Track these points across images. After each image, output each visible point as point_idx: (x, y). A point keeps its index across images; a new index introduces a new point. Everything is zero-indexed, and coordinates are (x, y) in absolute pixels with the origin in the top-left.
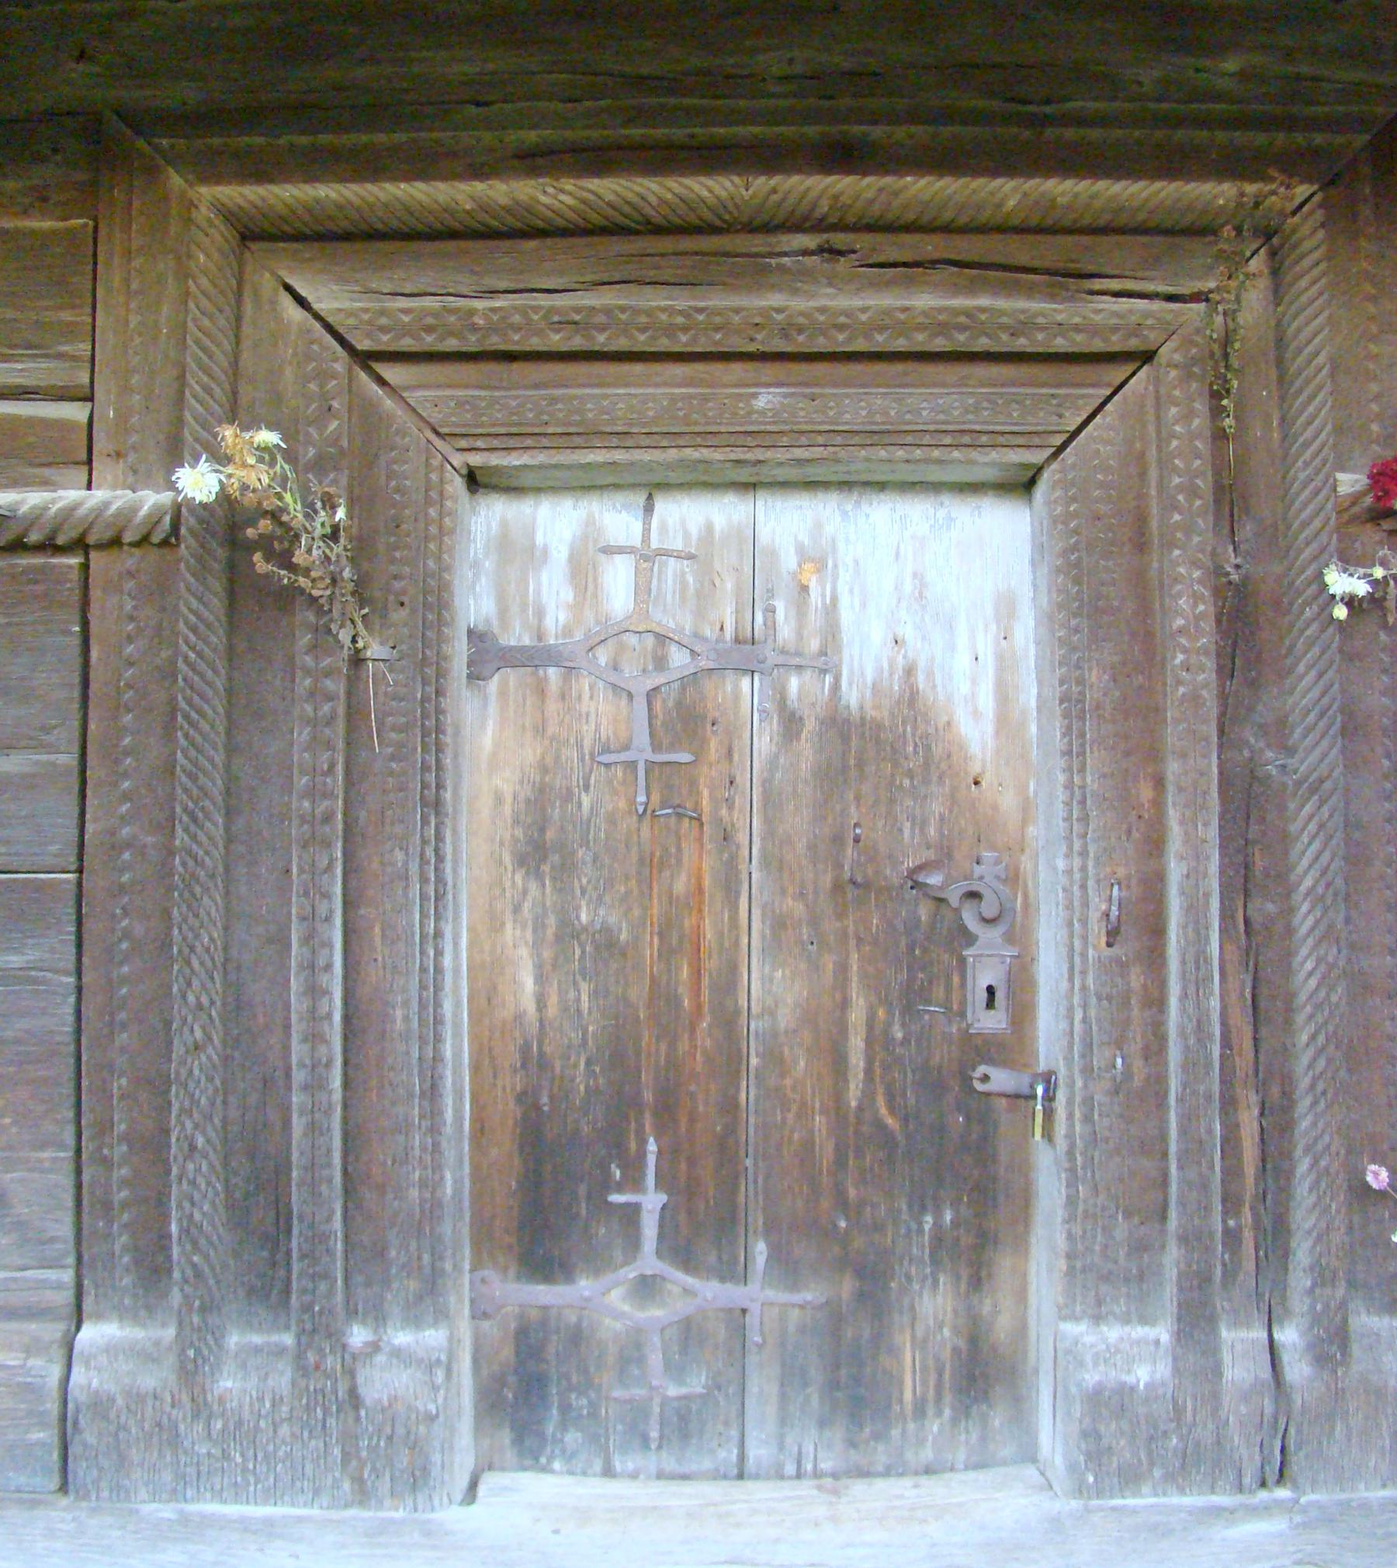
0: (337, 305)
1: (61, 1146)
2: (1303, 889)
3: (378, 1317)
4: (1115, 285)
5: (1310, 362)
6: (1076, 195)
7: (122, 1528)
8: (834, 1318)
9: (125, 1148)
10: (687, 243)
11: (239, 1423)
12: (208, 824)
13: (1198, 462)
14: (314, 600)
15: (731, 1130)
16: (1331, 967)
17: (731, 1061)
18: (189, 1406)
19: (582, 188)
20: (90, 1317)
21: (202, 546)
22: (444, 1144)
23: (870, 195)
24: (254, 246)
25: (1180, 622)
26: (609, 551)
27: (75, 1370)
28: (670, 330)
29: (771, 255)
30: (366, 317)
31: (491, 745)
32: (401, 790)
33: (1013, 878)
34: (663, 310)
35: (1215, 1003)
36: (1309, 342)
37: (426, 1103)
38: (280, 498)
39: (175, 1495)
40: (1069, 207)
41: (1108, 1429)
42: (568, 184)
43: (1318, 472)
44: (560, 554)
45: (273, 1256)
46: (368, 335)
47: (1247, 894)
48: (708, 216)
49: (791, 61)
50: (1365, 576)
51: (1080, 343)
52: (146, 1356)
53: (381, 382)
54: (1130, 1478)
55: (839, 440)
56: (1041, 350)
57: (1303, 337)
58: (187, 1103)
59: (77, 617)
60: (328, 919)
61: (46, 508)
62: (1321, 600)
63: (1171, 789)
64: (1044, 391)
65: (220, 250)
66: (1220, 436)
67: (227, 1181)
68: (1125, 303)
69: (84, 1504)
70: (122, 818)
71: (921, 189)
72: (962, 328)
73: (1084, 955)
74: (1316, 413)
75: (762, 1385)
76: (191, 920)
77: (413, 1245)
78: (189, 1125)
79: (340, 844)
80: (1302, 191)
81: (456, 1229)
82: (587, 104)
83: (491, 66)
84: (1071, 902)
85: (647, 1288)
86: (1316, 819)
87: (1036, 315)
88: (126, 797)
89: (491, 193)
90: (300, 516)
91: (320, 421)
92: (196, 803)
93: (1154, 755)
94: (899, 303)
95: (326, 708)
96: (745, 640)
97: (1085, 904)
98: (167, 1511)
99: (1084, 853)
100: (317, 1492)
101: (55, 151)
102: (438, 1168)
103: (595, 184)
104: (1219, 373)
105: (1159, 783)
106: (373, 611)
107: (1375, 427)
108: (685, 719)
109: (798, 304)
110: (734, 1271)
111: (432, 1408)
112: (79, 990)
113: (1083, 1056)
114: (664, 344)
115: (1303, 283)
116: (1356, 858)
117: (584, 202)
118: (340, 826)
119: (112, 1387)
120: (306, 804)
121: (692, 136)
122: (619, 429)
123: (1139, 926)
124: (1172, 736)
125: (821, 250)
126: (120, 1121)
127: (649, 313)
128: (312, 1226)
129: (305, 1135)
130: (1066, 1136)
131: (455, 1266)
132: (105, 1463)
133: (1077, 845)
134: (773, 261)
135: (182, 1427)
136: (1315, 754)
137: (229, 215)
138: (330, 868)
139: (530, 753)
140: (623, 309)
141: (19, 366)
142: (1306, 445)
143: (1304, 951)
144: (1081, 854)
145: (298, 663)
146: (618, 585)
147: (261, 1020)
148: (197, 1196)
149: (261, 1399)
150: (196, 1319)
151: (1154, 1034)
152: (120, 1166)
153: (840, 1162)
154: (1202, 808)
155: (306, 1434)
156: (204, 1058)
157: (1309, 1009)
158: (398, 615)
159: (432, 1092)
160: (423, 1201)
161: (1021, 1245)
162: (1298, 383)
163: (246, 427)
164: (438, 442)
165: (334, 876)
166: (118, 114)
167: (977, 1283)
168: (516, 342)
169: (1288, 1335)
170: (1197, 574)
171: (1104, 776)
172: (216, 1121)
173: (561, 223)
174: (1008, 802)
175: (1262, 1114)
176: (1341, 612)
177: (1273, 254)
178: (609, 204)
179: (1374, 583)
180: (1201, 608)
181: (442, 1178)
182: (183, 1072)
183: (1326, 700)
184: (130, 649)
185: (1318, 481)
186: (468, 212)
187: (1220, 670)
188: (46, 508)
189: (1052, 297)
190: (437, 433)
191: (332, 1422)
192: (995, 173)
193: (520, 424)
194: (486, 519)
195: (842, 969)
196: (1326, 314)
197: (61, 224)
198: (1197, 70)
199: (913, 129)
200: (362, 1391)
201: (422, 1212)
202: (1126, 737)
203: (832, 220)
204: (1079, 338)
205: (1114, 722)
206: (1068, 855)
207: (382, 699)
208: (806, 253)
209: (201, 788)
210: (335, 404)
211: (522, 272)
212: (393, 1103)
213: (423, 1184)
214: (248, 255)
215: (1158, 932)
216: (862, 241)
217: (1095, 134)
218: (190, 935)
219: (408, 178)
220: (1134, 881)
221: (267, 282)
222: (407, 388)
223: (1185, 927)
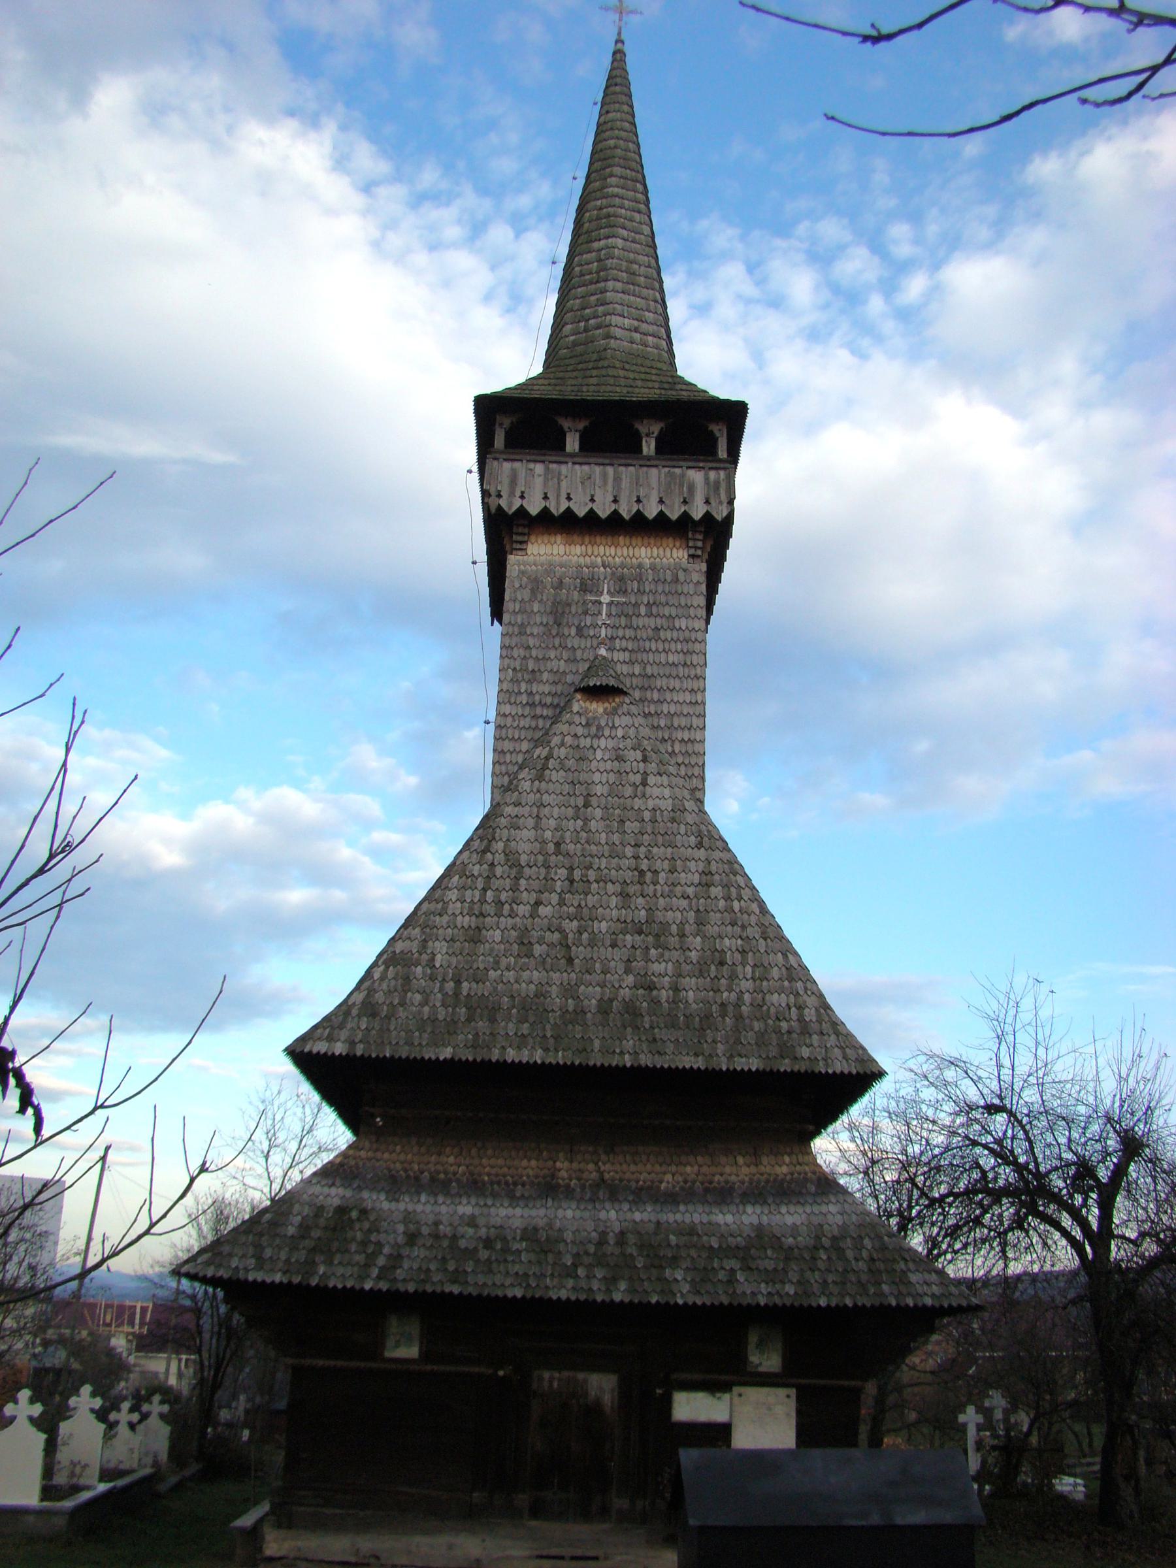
146: (555, 1384)
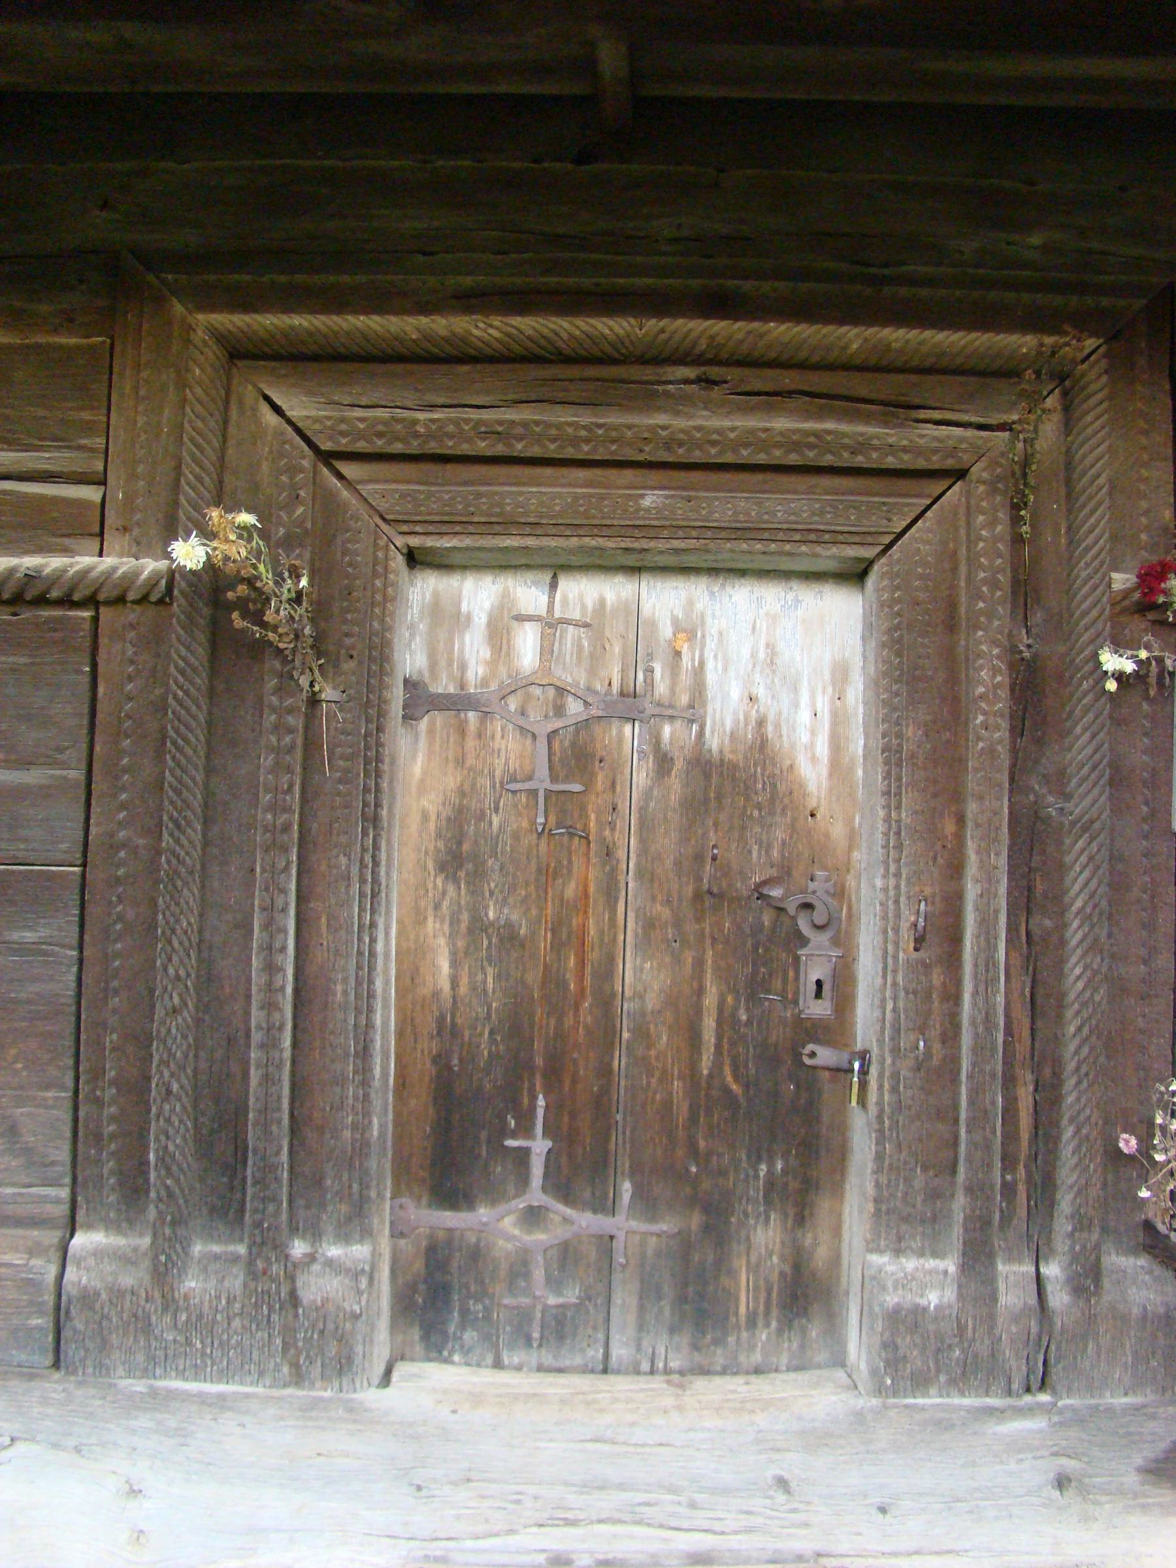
0: (305, 413)
1: (63, 1088)
2: (1074, 909)
3: (315, 1234)
4: (937, 415)
5: (1093, 482)
6: (907, 342)
7: (103, 1398)
8: (684, 1246)
9: (114, 1091)
10: (591, 371)
11: (200, 1317)
12: (189, 830)
13: (999, 561)
14: (280, 651)
15: (605, 1090)
16: (1095, 973)
17: (606, 1035)
18: (159, 1301)
19: (507, 324)
20: (81, 1227)
21: (191, 605)
22: (373, 1095)
23: (740, 336)
24: (240, 363)
25: (981, 690)
26: (521, 618)
27: (69, 1269)
28: (575, 442)
29: (659, 383)
30: (329, 423)
31: (420, 774)
32: (346, 807)
33: (840, 893)
34: (570, 424)
35: (1000, 999)
36: (1093, 466)
37: (359, 1062)
38: (255, 567)
39: (146, 1373)
40: (901, 351)
41: (904, 1342)
42: (496, 321)
43: (1096, 571)
44: (481, 619)
45: (231, 1181)
46: (331, 438)
47: (1029, 912)
48: (608, 349)
49: (679, 226)
50: (1132, 657)
51: (907, 461)
52: (126, 1260)
53: (340, 476)
54: (920, 1382)
55: (709, 534)
56: (875, 466)
57: (1087, 462)
58: (165, 1056)
59: (88, 660)
60: (284, 910)
61: (65, 571)
62: (1096, 676)
63: (970, 824)
64: (876, 499)
65: (212, 366)
66: (1018, 540)
67: (196, 1120)
68: (944, 431)
69: (72, 1378)
70: (120, 823)
71: (782, 333)
72: (811, 447)
73: (895, 957)
74: (1097, 524)
75: (624, 1297)
76: (173, 907)
77: (345, 1176)
78: (166, 1074)
79: (295, 850)
80: (1090, 343)
81: (381, 1164)
82: (514, 256)
83: (436, 224)
84: (886, 914)
85: (533, 1217)
86: (1086, 853)
87: (872, 437)
88: (123, 806)
89: (433, 326)
90: (271, 583)
91: (289, 506)
92: (180, 813)
93: (957, 797)
94: (761, 425)
95: (288, 739)
96: (628, 694)
97: (898, 916)
98: (139, 1386)
99: (898, 875)
100: (261, 1374)
101: (81, 281)
102: (367, 1114)
103: (517, 321)
104: (1018, 487)
105: (960, 819)
106: (327, 662)
107: (1144, 537)
108: (578, 757)
109: (680, 423)
110: (604, 1205)
111: (357, 1308)
112: (81, 961)
113: (892, 1039)
114: (569, 453)
115: (1089, 418)
116: (1118, 885)
117: (508, 335)
118: (296, 835)
119: (97, 1284)
120: (269, 817)
121: (598, 285)
122: (532, 520)
123: (940, 935)
124: (972, 782)
125: (698, 380)
126: (110, 1070)
127: (559, 426)
128: (263, 1158)
129: (260, 1084)
130: (877, 1103)
131: (378, 1194)
132: (90, 1345)
133: (892, 868)
134: (660, 388)
135: (154, 1318)
136: (1087, 800)
137: (221, 338)
138: (287, 868)
139: (452, 780)
140: (537, 423)
141: (47, 455)
142: (1088, 549)
143: (1074, 960)
144: (895, 875)
145: (266, 702)
146: (527, 646)
147: (228, 991)
148: (171, 1132)
149: (218, 1298)
150: (167, 1231)
151: (951, 1023)
152: (110, 1105)
153: (693, 1119)
154: (995, 840)
155: (254, 1327)
156: (180, 1020)
157: (1076, 1006)
158: (348, 666)
159: (364, 1052)
160: (354, 1140)
161: (838, 1190)
162: (1082, 499)
163: (229, 510)
164: (384, 527)
165: (289, 876)
166: (133, 253)
167: (801, 1220)
168: (450, 447)
169: (1052, 1270)
170: (996, 651)
171: (916, 812)
172: (189, 1071)
173: (488, 351)
174: (838, 831)
175: (1036, 1090)
176: (1111, 685)
177: (1065, 394)
178: (528, 337)
179: (1140, 663)
180: (999, 678)
181: (370, 1122)
182: (163, 1030)
183: (1097, 756)
184: (130, 687)
185: (1096, 579)
186: (414, 341)
187: (1012, 729)
188: (65, 571)
189: (886, 424)
190: (384, 520)
191: (275, 1317)
192: (842, 322)
193: (451, 514)
194: (421, 590)
195: (699, 963)
196: (1106, 444)
197: (84, 341)
198: (1008, 243)
199: (777, 284)
200: (300, 1293)
201: (353, 1149)
202: (935, 782)
203: (709, 356)
204: (906, 457)
205: (925, 769)
206: (885, 876)
207: (333, 733)
208: (687, 382)
209: (184, 801)
210: (302, 493)
211: (456, 391)
212: (333, 1061)
213: (355, 1127)
214: (234, 370)
215: (956, 940)
216: (732, 374)
217: (924, 292)
218: (172, 920)
219: (366, 312)
220: (938, 899)
221: (250, 392)
222: (361, 482)
223: (978, 937)
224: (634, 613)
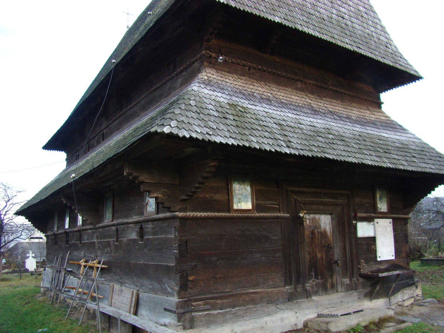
54: (348, 291)
75: (320, 288)
110: (318, 279)
224: (315, 217)
